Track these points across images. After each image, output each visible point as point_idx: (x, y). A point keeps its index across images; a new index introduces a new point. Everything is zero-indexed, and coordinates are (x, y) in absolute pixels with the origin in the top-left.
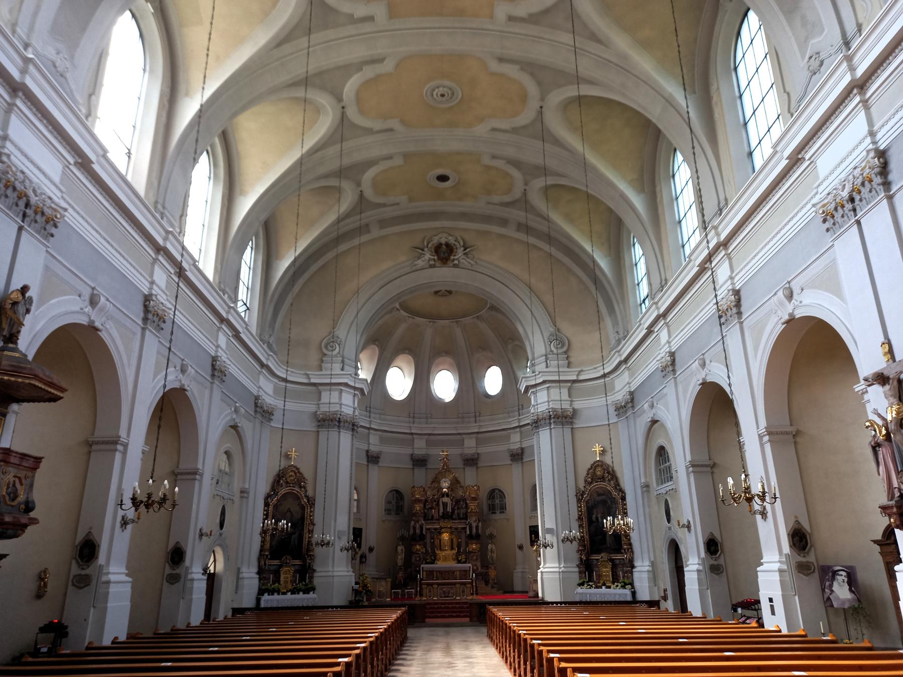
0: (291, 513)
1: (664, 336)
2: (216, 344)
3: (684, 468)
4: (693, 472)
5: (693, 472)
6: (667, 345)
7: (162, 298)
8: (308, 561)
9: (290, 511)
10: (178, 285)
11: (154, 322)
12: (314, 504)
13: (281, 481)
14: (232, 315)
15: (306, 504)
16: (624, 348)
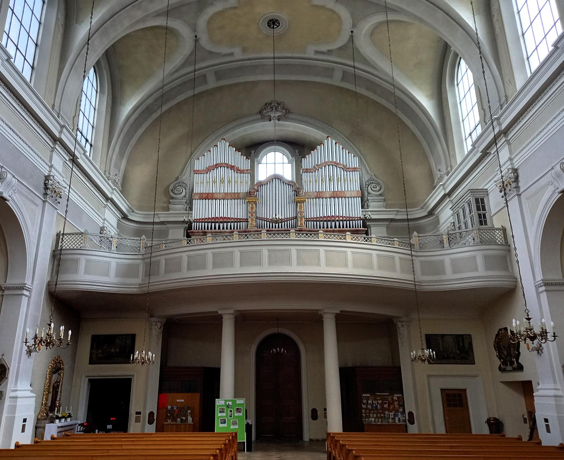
1: (504, 155)
2: (49, 164)
3: (534, 288)
4: (546, 291)
5: (546, 291)
6: (509, 162)
7: (58, 178)
10: (72, 169)
11: (52, 197)
14: (114, 195)
16: (448, 183)
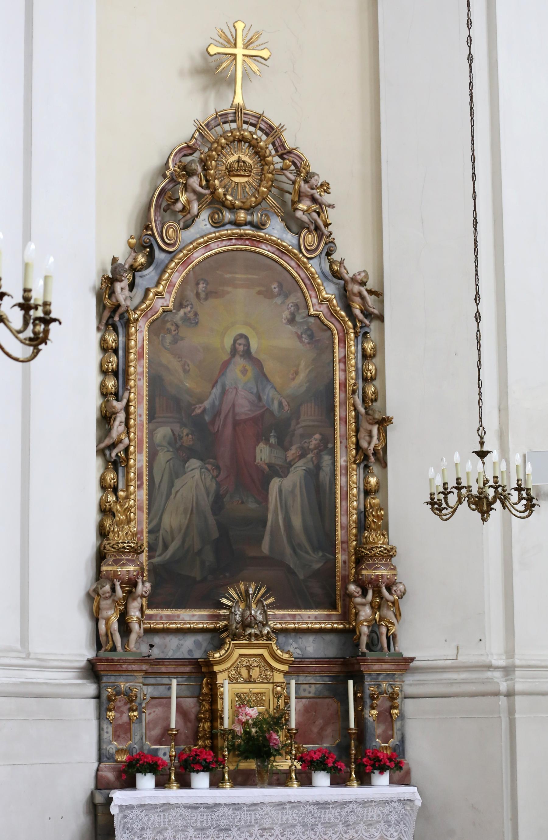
0: (258, 364)
8: (366, 613)
9: (247, 354)
12: (381, 318)
13: (183, 198)
15: (333, 314)
